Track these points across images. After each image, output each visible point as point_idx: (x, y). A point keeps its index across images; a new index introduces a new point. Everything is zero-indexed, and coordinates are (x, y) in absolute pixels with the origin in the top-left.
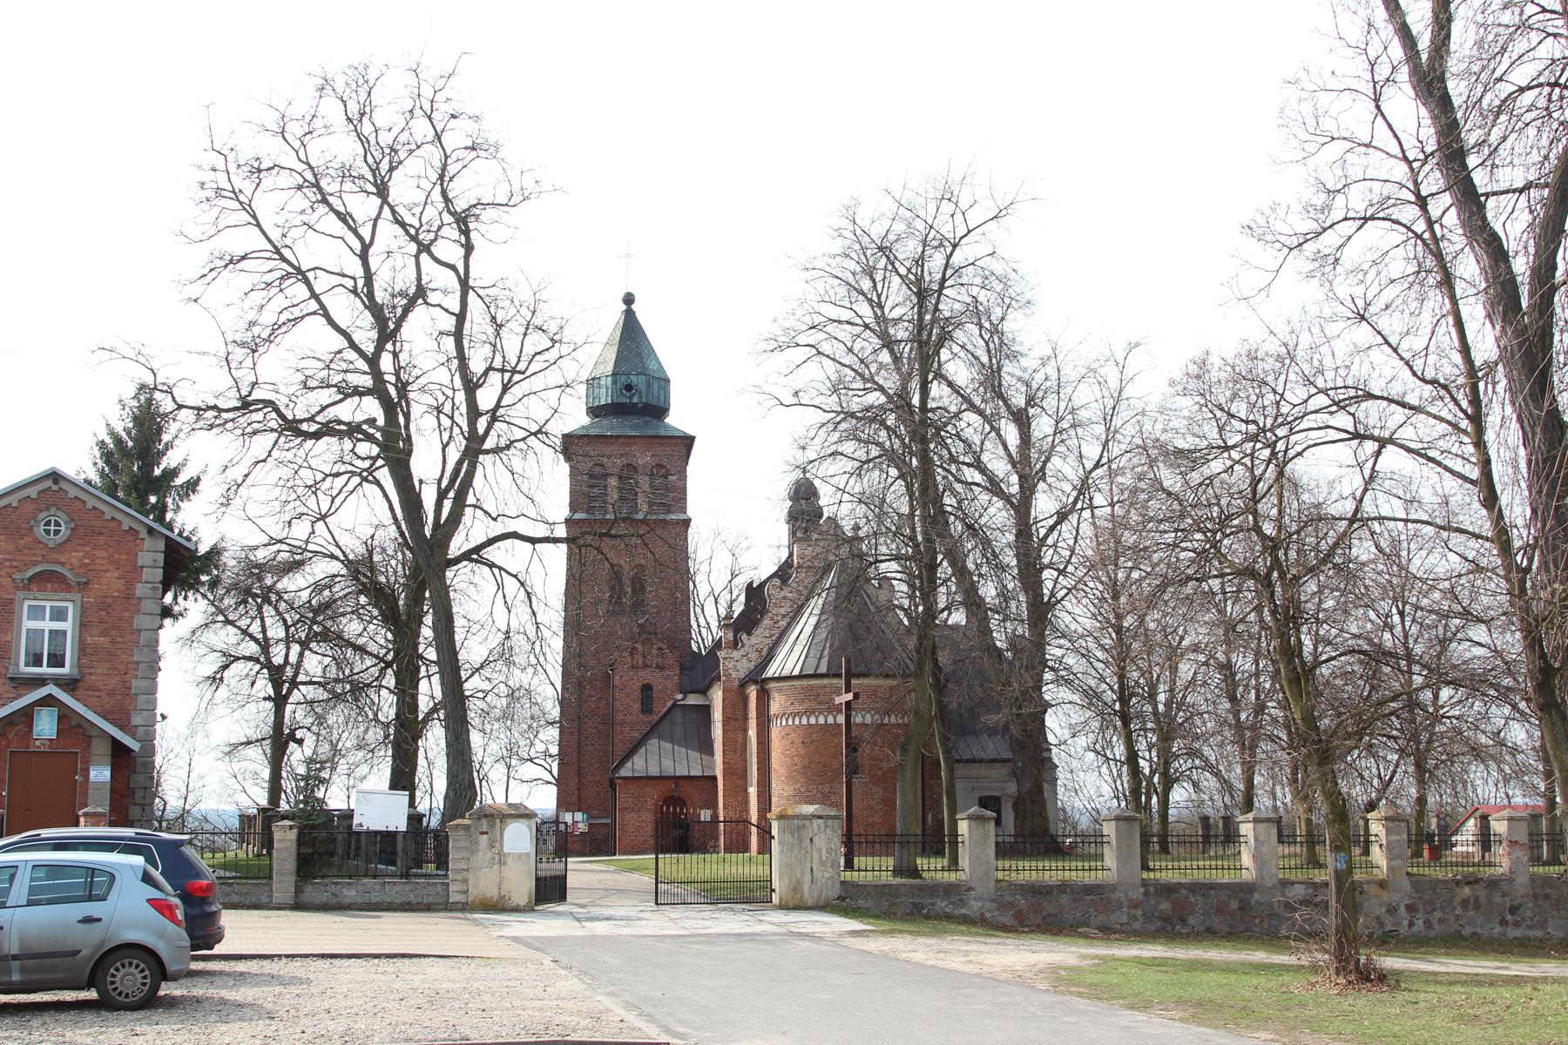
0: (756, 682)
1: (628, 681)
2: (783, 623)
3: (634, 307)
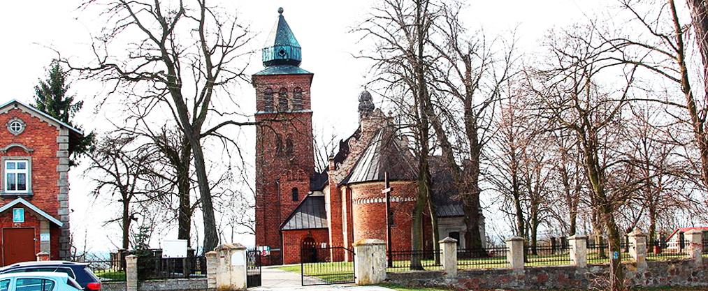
0: (345, 185)
2: (357, 158)
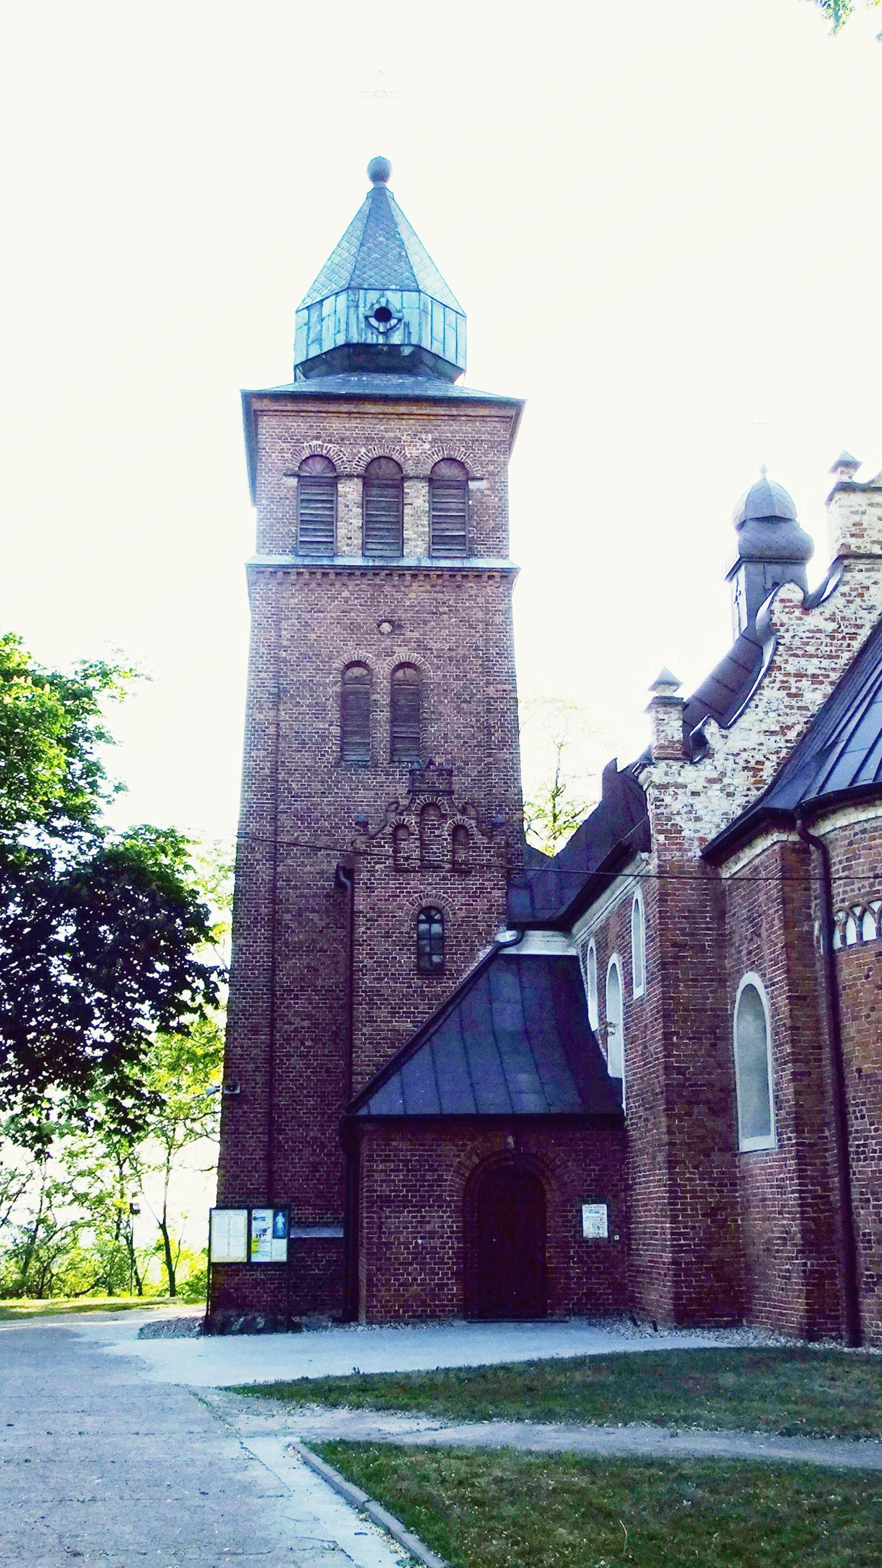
0: (781, 820)
1: (387, 901)
2: (815, 697)
3: (389, 185)
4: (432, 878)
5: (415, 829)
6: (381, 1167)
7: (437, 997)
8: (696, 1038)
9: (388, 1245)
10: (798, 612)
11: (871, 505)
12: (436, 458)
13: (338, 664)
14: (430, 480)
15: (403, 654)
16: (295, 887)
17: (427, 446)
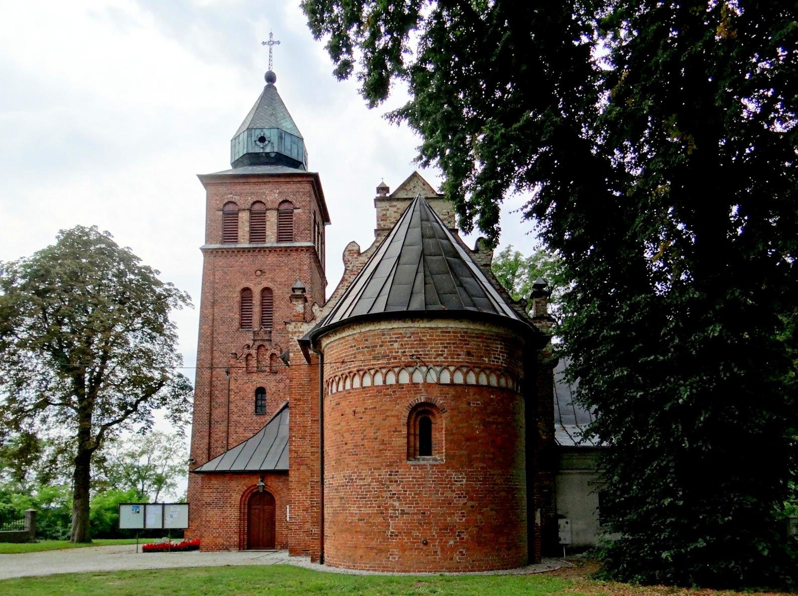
4: (262, 375)
5: (255, 355)
6: (207, 491)
7: (263, 423)
8: (303, 438)
9: (209, 521)
10: (355, 256)
11: (390, 206)
12: (281, 200)
13: (239, 289)
14: (278, 210)
15: (265, 284)
16: (220, 381)
17: (276, 195)
